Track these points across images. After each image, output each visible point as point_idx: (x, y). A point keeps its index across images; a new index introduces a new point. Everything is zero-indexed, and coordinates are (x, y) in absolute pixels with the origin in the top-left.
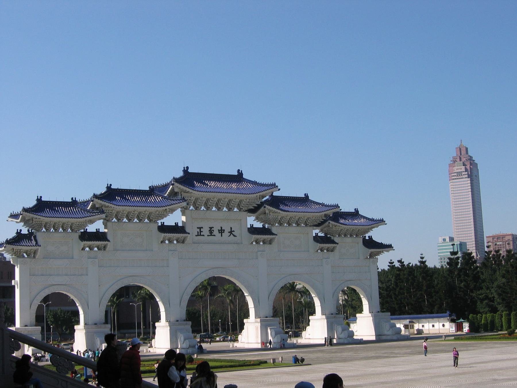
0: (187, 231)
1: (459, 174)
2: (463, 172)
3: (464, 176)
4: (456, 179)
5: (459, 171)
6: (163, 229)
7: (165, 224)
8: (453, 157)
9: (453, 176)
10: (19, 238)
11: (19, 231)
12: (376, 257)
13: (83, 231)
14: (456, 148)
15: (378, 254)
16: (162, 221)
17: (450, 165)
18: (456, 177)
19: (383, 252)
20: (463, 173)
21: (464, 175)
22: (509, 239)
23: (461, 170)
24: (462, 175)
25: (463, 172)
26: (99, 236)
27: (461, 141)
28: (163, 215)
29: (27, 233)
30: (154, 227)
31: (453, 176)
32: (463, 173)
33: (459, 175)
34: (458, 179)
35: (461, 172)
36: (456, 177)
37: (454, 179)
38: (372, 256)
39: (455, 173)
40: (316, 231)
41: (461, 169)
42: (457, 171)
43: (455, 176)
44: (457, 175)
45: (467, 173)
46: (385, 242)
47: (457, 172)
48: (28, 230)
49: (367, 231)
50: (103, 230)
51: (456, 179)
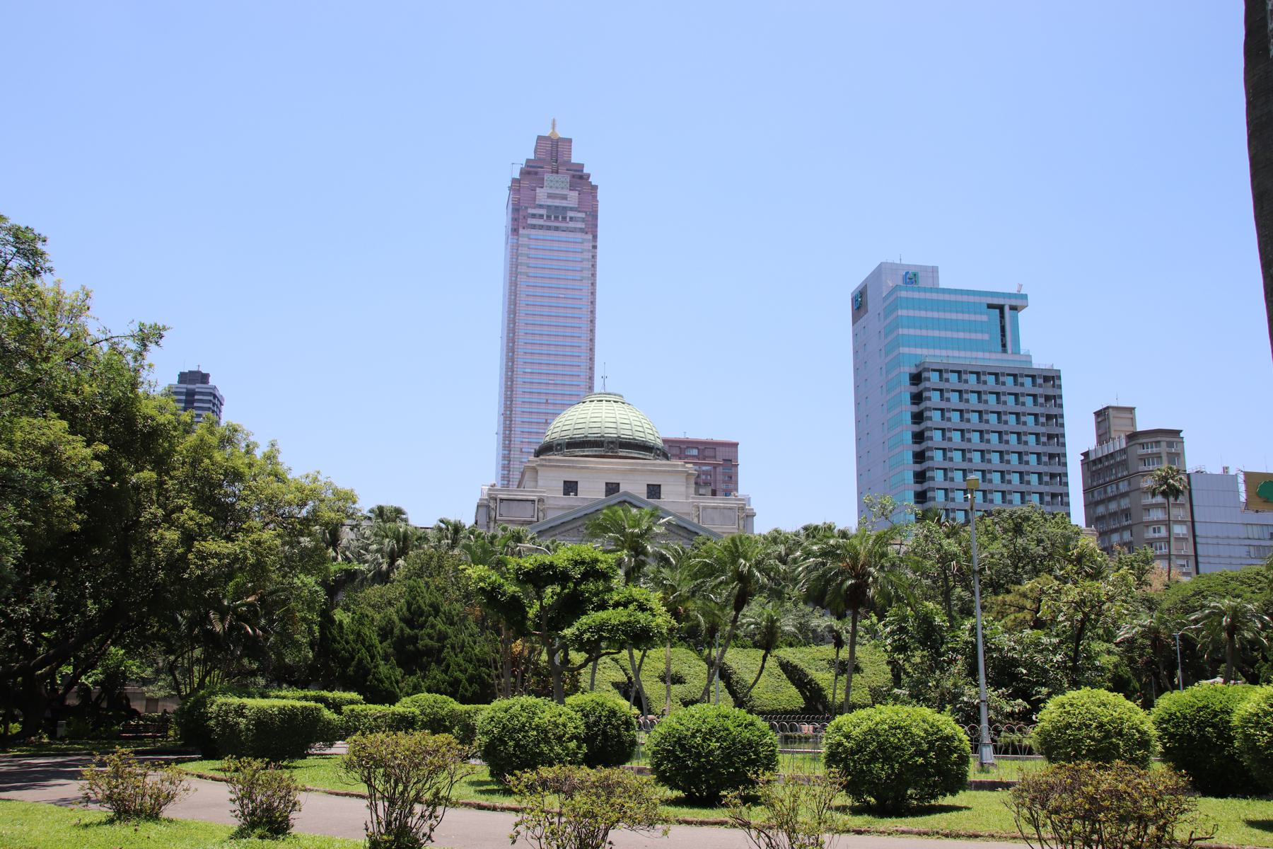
1: (558, 213)
2: (572, 209)
3: (572, 225)
4: (541, 227)
5: (557, 203)
8: (528, 161)
9: (534, 216)
14: (540, 138)
17: (516, 185)
18: (541, 222)
20: (570, 214)
21: (571, 219)
22: (727, 458)
23: (564, 203)
24: (564, 218)
25: (572, 209)
27: (554, 121)
31: (534, 216)
32: (570, 214)
33: (557, 218)
34: (549, 228)
35: (565, 209)
36: (541, 222)
37: (534, 227)
39: (541, 206)
41: (564, 198)
42: (550, 202)
43: (541, 216)
44: (549, 217)
45: (583, 215)
47: (549, 207)
51: (541, 227)
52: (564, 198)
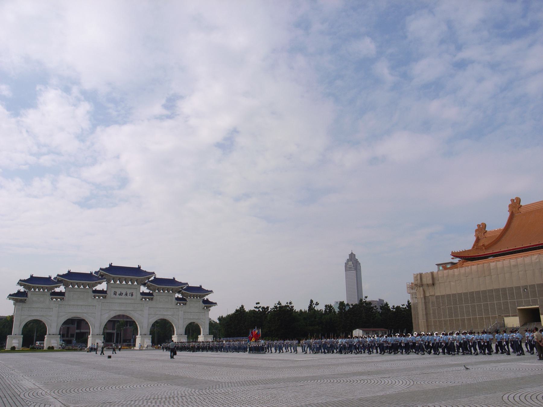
0: (107, 293)
6: (96, 291)
7: (97, 289)
10: (19, 293)
11: (19, 290)
12: (210, 308)
13: (53, 291)
15: (210, 307)
16: (96, 287)
19: (212, 306)
26: (61, 294)
28: (95, 285)
29: (23, 291)
30: (90, 291)
38: (208, 307)
40: (177, 295)
41: (351, 265)
46: (214, 302)
48: (24, 290)
49: (205, 296)
50: (63, 290)
52: (351, 265)
